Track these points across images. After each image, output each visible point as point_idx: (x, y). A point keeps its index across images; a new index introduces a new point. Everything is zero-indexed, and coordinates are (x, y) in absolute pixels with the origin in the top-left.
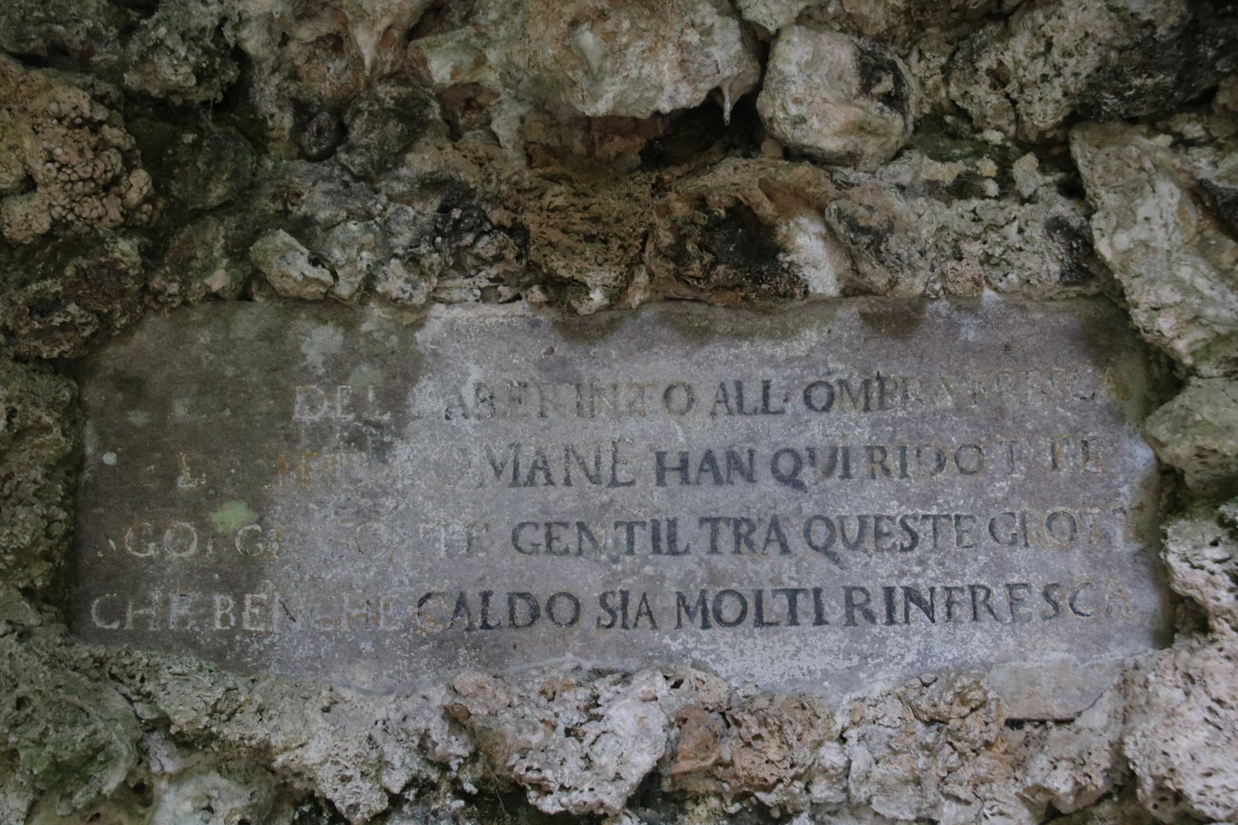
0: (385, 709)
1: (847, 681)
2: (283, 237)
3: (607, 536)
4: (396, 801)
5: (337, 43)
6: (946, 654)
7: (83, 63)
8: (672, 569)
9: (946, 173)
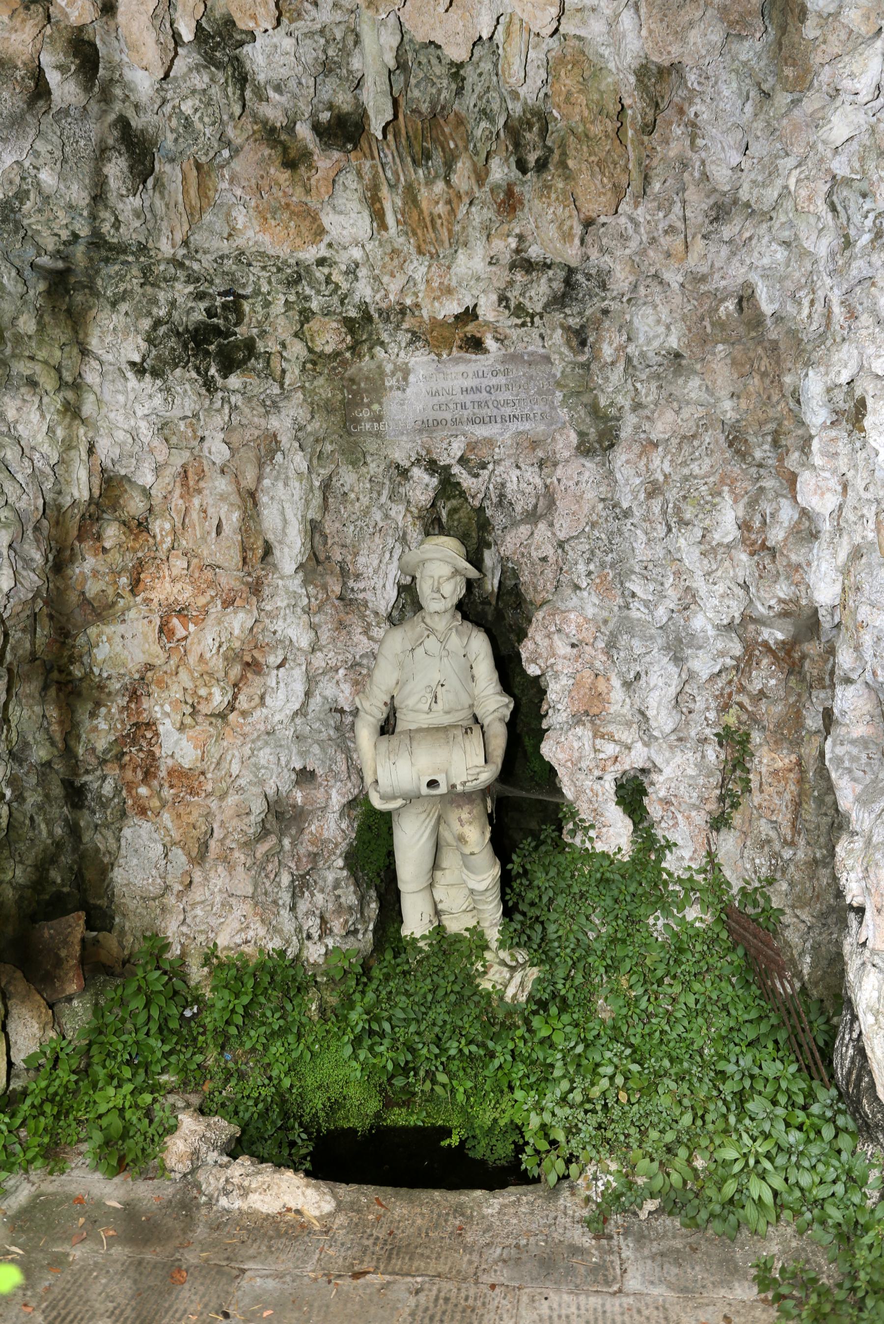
0: (409, 446)
1: (502, 434)
2: (378, 348)
3: (451, 406)
4: (413, 464)
5: (386, 296)
6: (521, 428)
7: (334, 313)
8: (465, 413)
9: (519, 321)
